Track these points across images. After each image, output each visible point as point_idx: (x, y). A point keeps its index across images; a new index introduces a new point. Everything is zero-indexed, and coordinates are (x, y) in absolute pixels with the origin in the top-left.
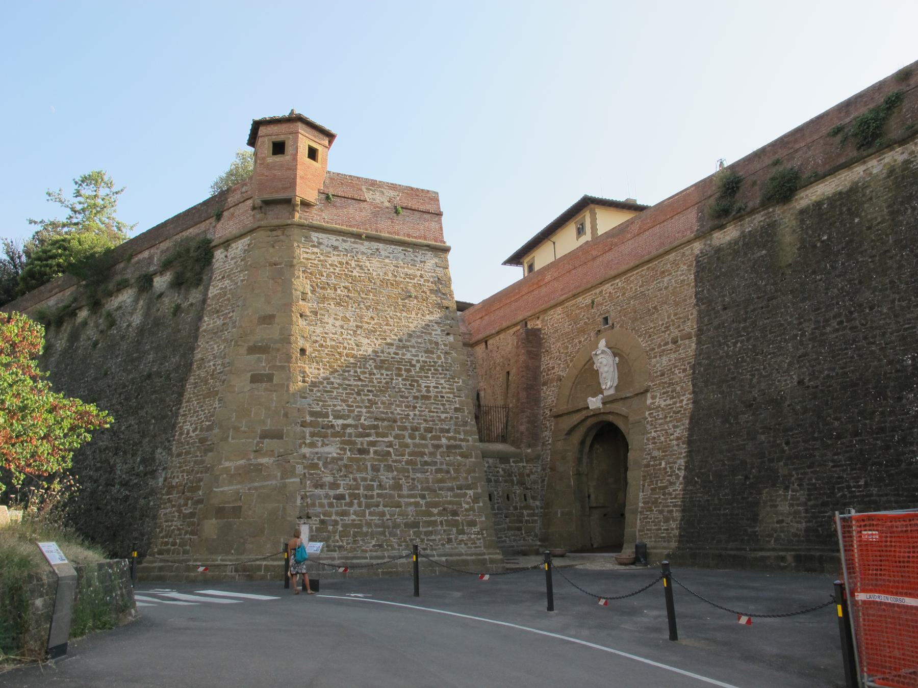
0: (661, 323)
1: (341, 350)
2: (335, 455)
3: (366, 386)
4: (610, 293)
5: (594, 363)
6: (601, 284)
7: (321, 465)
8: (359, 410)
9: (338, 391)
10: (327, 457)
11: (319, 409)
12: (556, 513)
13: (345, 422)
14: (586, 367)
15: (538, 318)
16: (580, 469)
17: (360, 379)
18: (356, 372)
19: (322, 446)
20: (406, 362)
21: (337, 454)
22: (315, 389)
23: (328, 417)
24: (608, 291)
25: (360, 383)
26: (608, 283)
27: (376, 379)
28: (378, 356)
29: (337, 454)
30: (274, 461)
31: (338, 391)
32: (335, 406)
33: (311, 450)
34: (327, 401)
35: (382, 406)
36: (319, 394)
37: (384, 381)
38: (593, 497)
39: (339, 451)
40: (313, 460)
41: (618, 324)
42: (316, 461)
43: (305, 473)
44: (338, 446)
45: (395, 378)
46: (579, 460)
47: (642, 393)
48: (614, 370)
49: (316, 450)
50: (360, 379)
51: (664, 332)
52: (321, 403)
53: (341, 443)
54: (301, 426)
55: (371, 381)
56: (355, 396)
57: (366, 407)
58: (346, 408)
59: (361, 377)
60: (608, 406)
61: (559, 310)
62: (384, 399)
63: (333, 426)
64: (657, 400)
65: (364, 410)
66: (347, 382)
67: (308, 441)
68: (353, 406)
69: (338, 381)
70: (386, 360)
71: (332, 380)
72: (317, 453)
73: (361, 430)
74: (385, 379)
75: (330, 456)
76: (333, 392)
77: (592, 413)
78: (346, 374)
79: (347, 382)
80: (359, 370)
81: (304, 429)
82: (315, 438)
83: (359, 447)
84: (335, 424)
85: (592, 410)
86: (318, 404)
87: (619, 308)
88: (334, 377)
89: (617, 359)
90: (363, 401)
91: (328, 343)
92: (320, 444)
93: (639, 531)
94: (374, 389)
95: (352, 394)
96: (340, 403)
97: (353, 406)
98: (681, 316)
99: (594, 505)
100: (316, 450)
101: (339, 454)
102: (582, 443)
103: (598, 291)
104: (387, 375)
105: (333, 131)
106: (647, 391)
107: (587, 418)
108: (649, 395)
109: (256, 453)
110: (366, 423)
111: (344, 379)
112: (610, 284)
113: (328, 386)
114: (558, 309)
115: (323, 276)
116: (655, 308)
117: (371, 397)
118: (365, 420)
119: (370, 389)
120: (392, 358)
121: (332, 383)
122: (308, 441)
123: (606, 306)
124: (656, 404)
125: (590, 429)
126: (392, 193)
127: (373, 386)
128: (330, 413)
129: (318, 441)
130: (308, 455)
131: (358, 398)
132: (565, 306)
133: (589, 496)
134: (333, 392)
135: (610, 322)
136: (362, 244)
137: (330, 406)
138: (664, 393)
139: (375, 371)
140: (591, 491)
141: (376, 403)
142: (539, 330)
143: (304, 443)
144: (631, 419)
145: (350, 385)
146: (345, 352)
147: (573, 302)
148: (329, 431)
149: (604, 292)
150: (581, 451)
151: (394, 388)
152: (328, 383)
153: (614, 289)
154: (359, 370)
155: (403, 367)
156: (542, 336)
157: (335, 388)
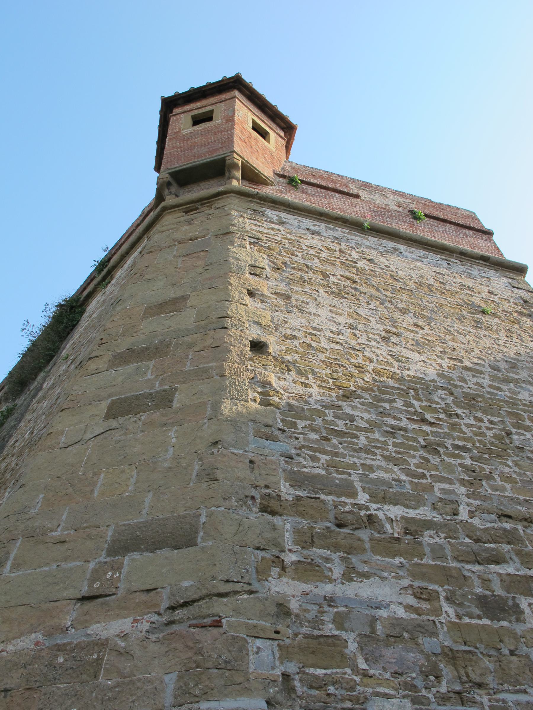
1: (360, 360)
2: (401, 612)
3: (446, 436)
7: (352, 647)
8: (447, 486)
9: (371, 436)
10: (374, 620)
11: (323, 472)
13: (412, 513)
17: (424, 421)
18: (409, 405)
19: (347, 577)
20: (525, 405)
21: (409, 608)
22: (301, 424)
23: (353, 494)
25: (428, 429)
27: (469, 426)
28: (456, 386)
29: (409, 608)
30: (154, 629)
31: (371, 436)
32: (370, 468)
33: (306, 587)
34: (344, 456)
35: (508, 486)
36: (315, 436)
37: (490, 433)
39: (411, 601)
40: (317, 623)
42: (330, 629)
43: (286, 676)
44: (406, 582)
45: (513, 430)
49: (328, 589)
50: (424, 421)
52: (324, 458)
53: (414, 576)
54: (264, 509)
55: (454, 427)
56: (422, 452)
57: (463, 482)
58: (403, 477)
59: (428, 416)
62: (507, 469)
63: (371, 520)
65: (462, 490)
66: (391, 421)
67: (290, 558)
68: (423, 476)
69: (366, 416)
70: (479, 396)
71: (349, 411)
72: (330, 601)
73: (467, 540)
74: (488, 429)
75: (383, 613)
76: (357, 437)
78: (386, 405)
79: (391, 421)
80: (416, 404)
81: (277, 520)
82: (317, 552)
83: (479, 590)
84: (380, 514)
86: (314, 459)
88: (353, 407)
90: (450, 468)
91: (324, 343)
92: (337, 571)
94: (469, 445)
95: (415, 449)
96: (383, 464)
97: (423, 476)
100: (328, 589)
101: (417, 611)
104: (491, 422)
105: (293, 120)
109: (89, 606)
110: (476, 521)
111: (382, 414)
113: (341, 423)
115: (297, 256)
117: (468, 462)
118: (472, 514)
119: (460, 443)
120: (488, 393)
121: (352, 419)
122: (294, 558)
126: (401, 200)
127: (465, 439)
128: (358, 486)
129: (327, 560)
130: (294, 606)
131: (434, 460)
134: (357, 437)
136: (366, 239)
137: (353, 466)
139: (459, 411)
141: (489, 477)
143: (278, 562)
145: (401, 429)
146: (370, 367)
148: (364, 535)
151: (521, 449)
152: (336, 416)
154: (416, 404)
155: (526, 415)
157: (359, 429)
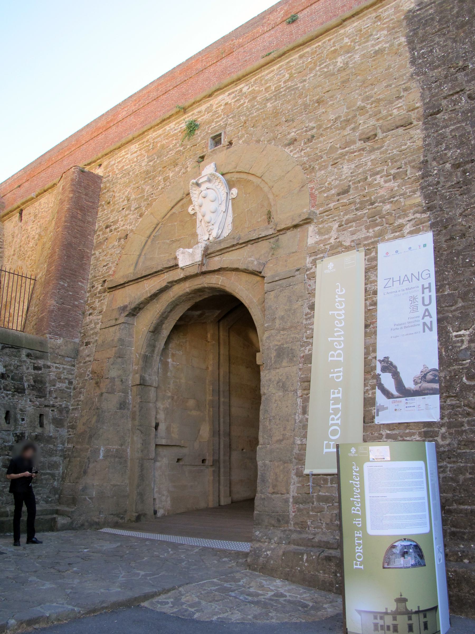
0: (332, 117)
4: (226, 104)
5: (190, 202)
6: (210, 96)
12: (97, 451)
14: (173, 210)
15: (100, 165)
16: (147, 378)
24: (223, 103)
26: (224, 93)
38: (162, 427)
41: (239, 139)
46: (147, 359)
47: (296, 226)
48: (226, 211)
51: (343, 128)
60: (217, 259)
61: (134, 147)
64: (334, 234)
77: (182, 275)
85: (182, 269)
87: (243, 119)
89: (235, 191)
93: (296, 501)
98: (381, 97)
99: (164, 442)
102: (156, 330)
103: (203, 108)
106: (308, 221)
107: (172, 284)
108: (311, 228)
112: (227, 94)
114: (133, 147)
116: (319, 102)
123: (217, 122)
124: (332, 241)
125: (174, 305)
132: (145, 140)
133: (157, 427)
135: (225, 141)
138: (348, 222)
140: (161, 416)
142: (100, 178)
144: (268, 273)
147: (160, 132)
149: (215, 107)
150: (152, 346)
153: (234, 98)
156: (102, 186)
